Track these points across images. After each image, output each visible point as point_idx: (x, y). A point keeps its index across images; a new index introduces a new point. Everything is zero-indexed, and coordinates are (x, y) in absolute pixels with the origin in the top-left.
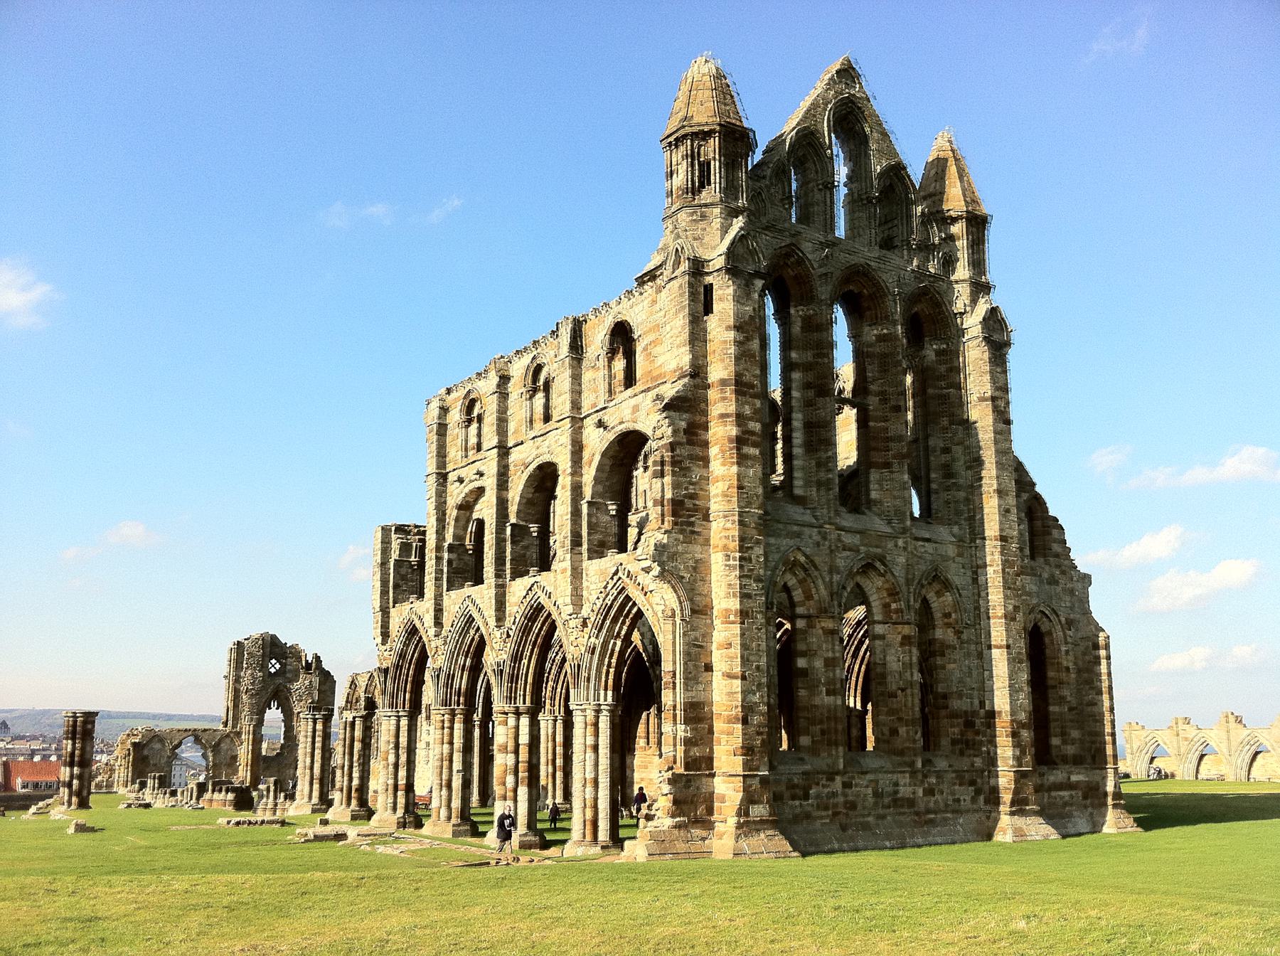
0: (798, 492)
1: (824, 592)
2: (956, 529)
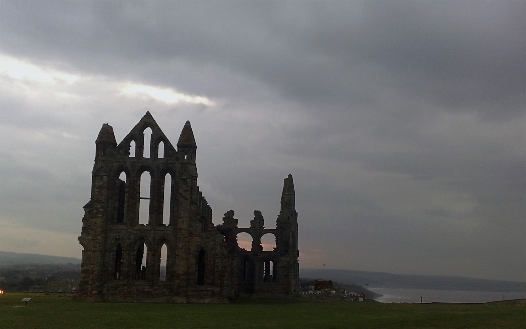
0: (124, 222)
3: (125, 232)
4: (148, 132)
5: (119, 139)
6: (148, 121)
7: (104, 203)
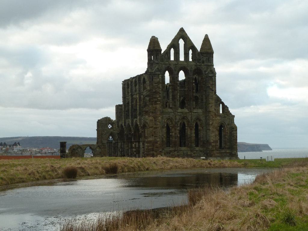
0: (171, 106)
1: (174, 123)
2: (203, 110)
3: (173, 114)
4: (181, 42)
5: (164, 47)
6: (182, 34)
7: (160, 94)
